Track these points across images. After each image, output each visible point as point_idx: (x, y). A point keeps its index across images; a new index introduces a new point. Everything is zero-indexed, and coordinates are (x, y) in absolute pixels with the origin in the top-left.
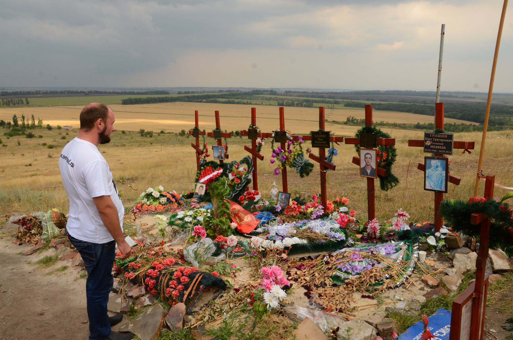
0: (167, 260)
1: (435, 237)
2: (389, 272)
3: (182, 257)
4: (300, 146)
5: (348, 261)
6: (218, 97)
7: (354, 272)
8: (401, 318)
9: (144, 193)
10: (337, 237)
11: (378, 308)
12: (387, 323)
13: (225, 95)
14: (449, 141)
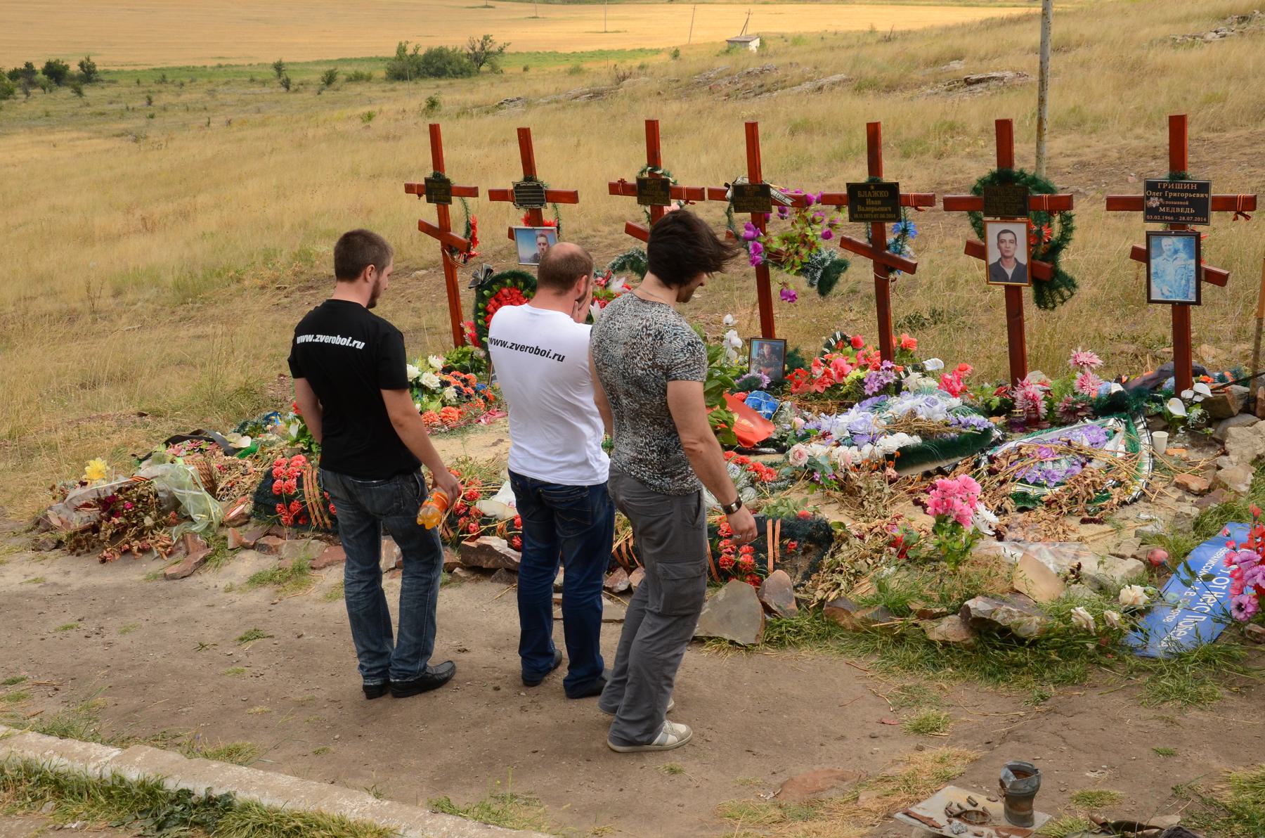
1: (1183, 400)
7: (1050, 481)
10: (975, 423)
14: (1202, 195)
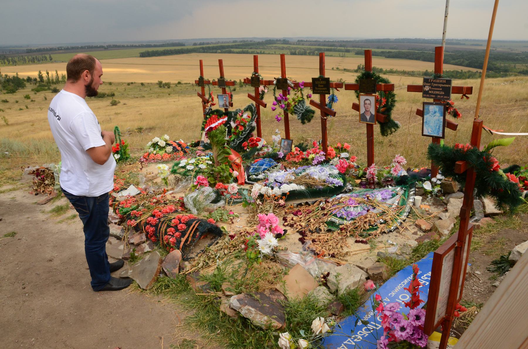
0: (167, 208)
1: (432, 182)
2: (384, 217)
3: (183, 205)
4: (301, 93)
5: (343, 207)
6: (232, 47)
7: (349, 217)
8: (392, 263)
9: (150, 142)
10: (335, 183)
11: (371, 252)
12: (377, 267)
13: (239, 45)
14: (448, 86)
